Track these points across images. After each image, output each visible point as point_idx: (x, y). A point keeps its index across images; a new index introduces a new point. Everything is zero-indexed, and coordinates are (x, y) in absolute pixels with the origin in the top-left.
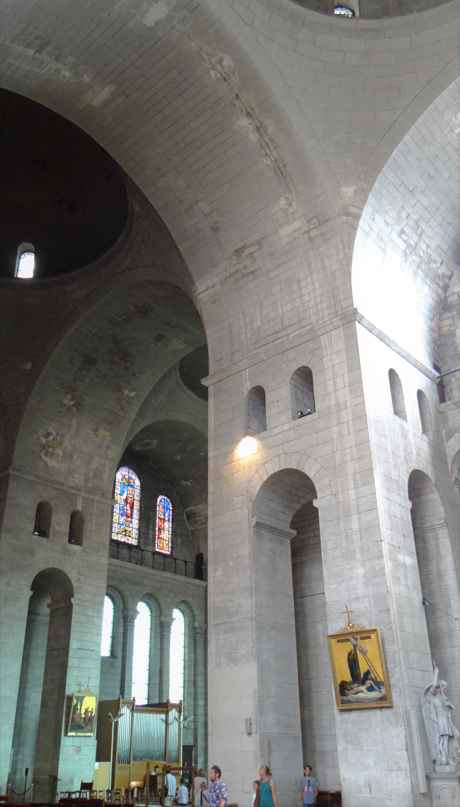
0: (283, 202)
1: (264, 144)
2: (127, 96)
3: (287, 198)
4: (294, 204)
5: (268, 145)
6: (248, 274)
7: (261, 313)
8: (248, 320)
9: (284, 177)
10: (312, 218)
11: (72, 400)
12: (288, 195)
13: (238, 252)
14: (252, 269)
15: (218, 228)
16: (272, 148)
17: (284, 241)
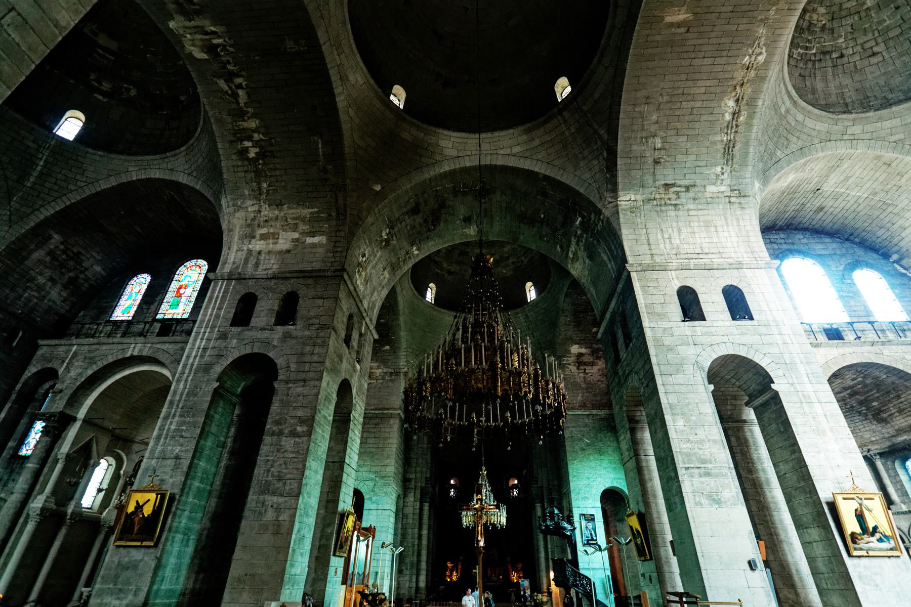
0: (719, 169)
1: (730, 125)
2: (688, 31)
3: (723, 168)
4: (726, 174)
5: (732, 128)
6: (671, 205)
7: (680, 235)
8: (666, 236)
9: (728, 154)
10: (735, 190)
11: (387, 235)
12: (724, 167)
13: (667, 186)
14: (675, 202)
15: (659, 162)
16: (733, 131)
17: (708, 195)
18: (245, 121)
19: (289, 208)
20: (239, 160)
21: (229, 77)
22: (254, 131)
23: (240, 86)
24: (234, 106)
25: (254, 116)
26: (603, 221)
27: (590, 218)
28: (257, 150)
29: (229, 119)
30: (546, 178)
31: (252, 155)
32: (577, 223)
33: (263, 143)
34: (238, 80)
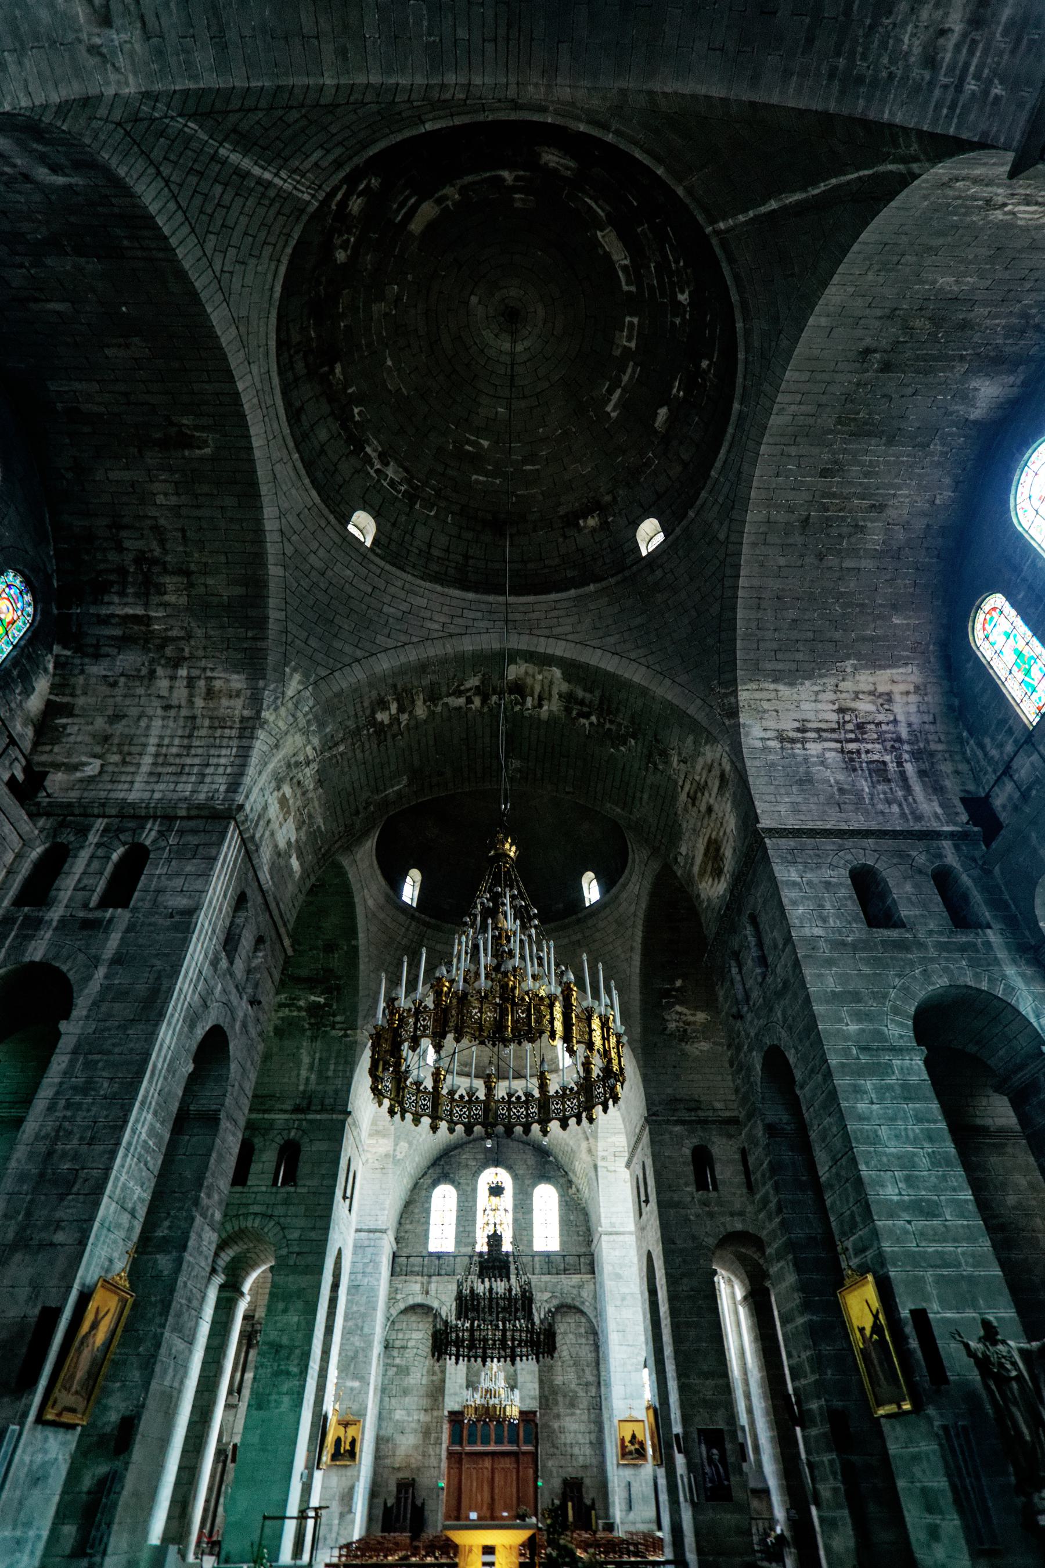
18: (425, 702)
19: (319, 798)
20: (371, 703)
21: (483, 692)
22: (411, 713)
23: (469, 701)
24: (444, 689)
25: (432, 714)
26: (346, 1036)
27: (334, 1016)
28: (387, 722)
29: (425, 682)
30: (355, 949)
31: (382, 717)
32: (313, 998)
33: (395, 727)
34: (477, 701)
